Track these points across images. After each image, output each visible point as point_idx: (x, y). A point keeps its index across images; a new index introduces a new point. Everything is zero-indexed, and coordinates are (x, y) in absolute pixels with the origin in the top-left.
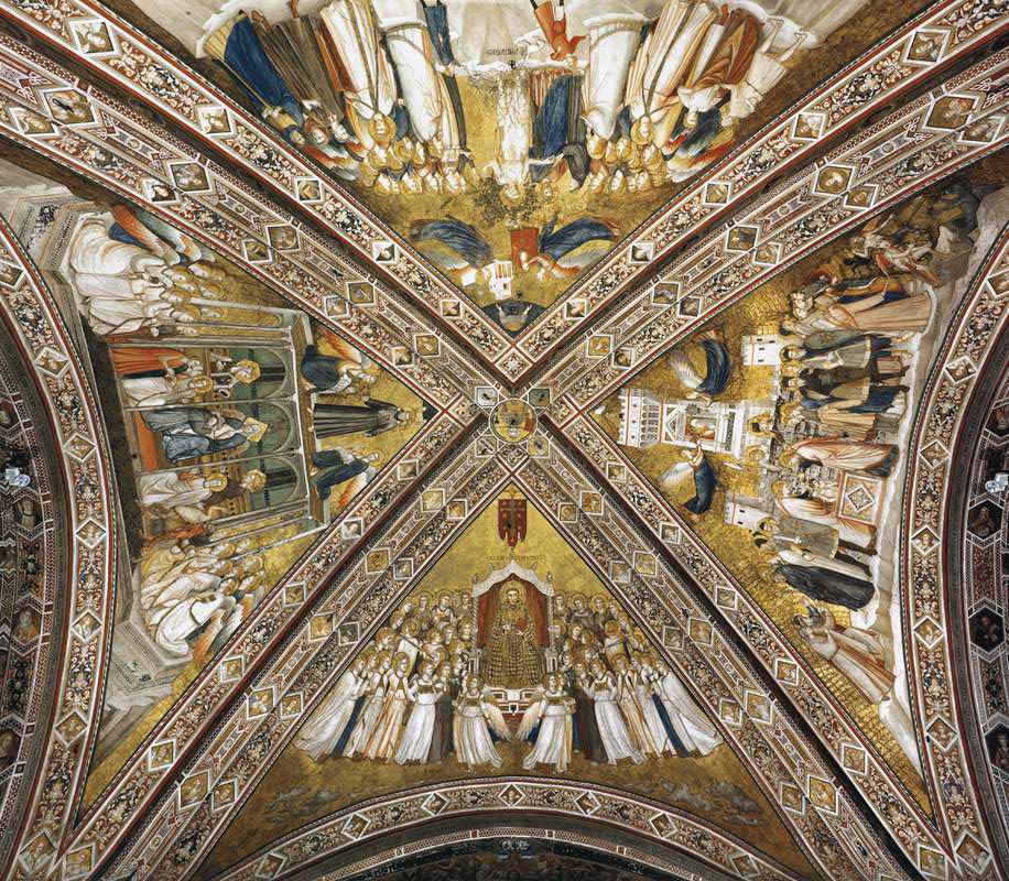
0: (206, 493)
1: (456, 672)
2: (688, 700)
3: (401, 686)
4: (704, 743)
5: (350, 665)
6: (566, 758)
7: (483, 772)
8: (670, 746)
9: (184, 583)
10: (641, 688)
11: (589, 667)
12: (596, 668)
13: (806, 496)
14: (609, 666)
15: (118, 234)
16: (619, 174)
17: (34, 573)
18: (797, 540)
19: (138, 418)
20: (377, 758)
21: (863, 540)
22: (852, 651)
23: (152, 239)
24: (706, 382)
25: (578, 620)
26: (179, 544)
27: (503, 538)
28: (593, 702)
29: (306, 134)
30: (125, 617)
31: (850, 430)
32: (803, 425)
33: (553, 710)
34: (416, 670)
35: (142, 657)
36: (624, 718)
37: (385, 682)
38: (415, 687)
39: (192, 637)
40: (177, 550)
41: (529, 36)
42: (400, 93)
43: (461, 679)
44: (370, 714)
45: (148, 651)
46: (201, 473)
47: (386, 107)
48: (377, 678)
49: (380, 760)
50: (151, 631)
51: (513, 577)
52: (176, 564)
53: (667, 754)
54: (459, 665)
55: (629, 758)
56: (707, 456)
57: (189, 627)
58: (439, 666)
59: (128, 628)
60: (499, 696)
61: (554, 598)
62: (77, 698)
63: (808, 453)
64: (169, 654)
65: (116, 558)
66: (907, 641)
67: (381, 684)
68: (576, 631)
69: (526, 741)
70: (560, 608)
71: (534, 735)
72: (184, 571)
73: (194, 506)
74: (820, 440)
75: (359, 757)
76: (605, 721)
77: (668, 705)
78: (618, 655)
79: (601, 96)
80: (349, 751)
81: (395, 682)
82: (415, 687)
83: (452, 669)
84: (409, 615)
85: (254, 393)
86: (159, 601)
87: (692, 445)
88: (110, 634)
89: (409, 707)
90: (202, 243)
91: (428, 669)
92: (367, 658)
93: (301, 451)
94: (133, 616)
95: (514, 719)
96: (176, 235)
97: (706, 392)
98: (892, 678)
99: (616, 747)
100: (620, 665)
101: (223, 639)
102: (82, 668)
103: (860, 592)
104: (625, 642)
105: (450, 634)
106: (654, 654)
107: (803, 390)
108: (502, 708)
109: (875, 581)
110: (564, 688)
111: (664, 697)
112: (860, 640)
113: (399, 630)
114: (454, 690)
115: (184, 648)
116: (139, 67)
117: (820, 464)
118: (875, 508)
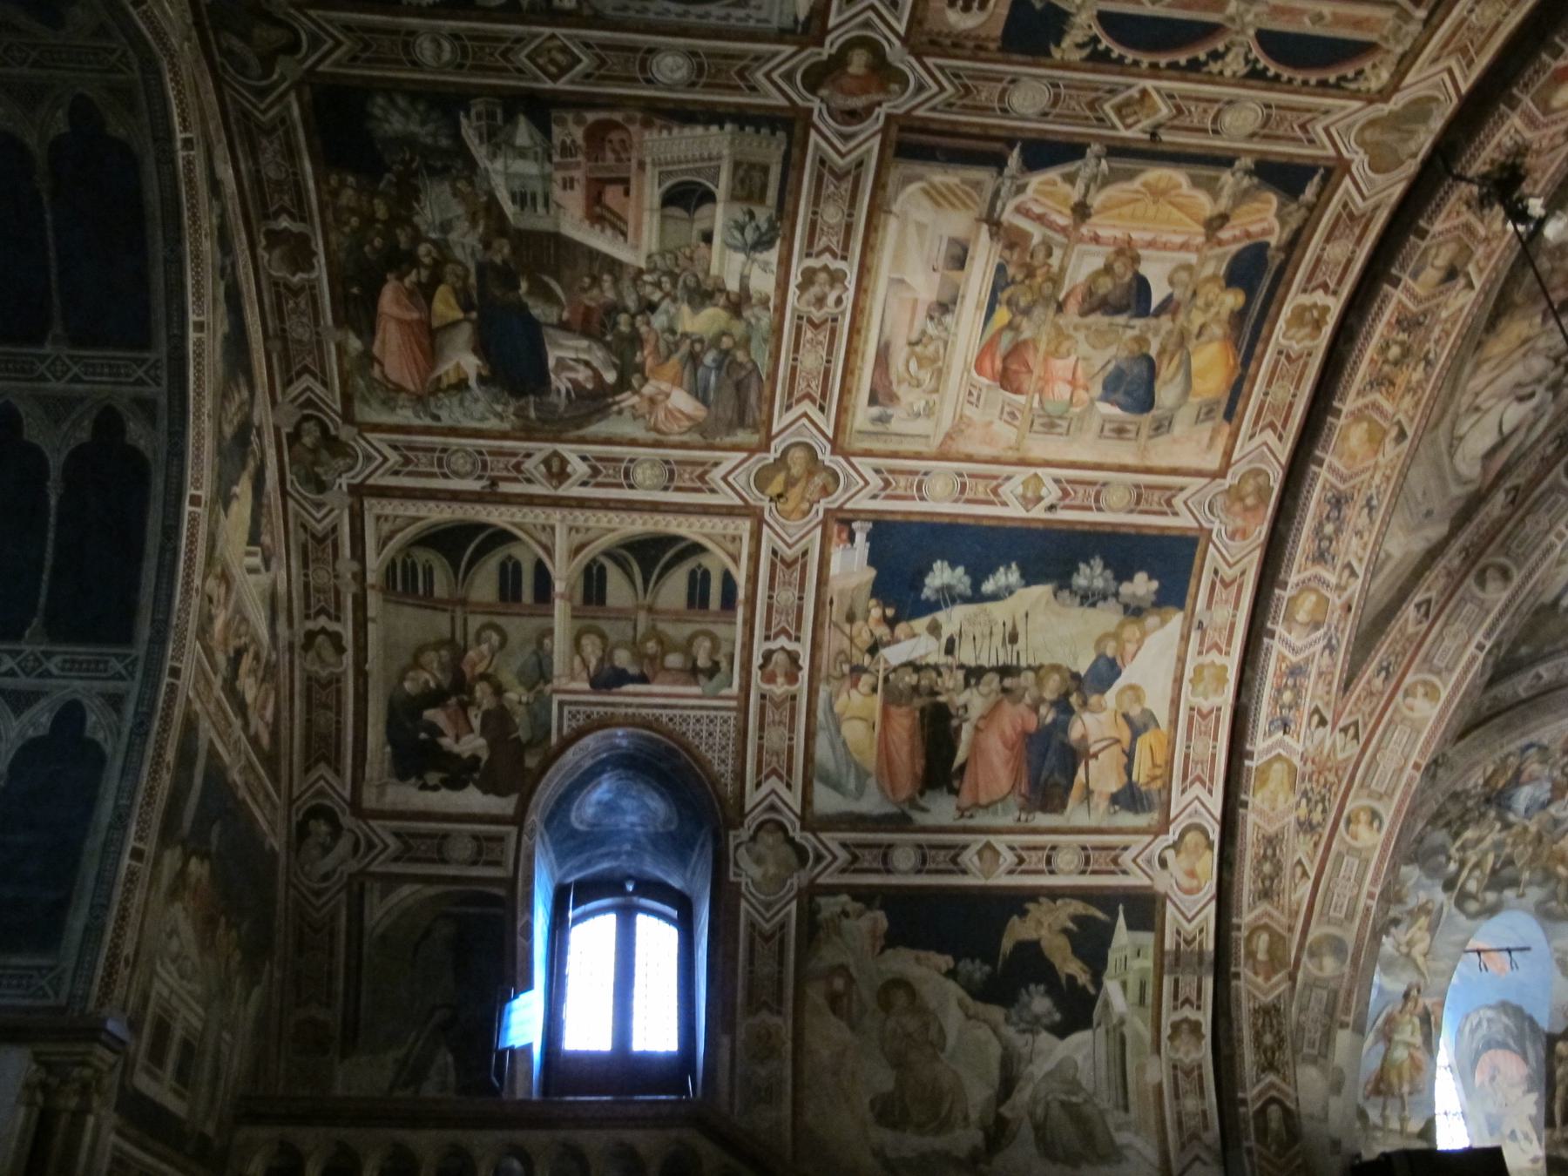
17: (1396, 363)
30: (1436, 425)
86: (1479, 400)
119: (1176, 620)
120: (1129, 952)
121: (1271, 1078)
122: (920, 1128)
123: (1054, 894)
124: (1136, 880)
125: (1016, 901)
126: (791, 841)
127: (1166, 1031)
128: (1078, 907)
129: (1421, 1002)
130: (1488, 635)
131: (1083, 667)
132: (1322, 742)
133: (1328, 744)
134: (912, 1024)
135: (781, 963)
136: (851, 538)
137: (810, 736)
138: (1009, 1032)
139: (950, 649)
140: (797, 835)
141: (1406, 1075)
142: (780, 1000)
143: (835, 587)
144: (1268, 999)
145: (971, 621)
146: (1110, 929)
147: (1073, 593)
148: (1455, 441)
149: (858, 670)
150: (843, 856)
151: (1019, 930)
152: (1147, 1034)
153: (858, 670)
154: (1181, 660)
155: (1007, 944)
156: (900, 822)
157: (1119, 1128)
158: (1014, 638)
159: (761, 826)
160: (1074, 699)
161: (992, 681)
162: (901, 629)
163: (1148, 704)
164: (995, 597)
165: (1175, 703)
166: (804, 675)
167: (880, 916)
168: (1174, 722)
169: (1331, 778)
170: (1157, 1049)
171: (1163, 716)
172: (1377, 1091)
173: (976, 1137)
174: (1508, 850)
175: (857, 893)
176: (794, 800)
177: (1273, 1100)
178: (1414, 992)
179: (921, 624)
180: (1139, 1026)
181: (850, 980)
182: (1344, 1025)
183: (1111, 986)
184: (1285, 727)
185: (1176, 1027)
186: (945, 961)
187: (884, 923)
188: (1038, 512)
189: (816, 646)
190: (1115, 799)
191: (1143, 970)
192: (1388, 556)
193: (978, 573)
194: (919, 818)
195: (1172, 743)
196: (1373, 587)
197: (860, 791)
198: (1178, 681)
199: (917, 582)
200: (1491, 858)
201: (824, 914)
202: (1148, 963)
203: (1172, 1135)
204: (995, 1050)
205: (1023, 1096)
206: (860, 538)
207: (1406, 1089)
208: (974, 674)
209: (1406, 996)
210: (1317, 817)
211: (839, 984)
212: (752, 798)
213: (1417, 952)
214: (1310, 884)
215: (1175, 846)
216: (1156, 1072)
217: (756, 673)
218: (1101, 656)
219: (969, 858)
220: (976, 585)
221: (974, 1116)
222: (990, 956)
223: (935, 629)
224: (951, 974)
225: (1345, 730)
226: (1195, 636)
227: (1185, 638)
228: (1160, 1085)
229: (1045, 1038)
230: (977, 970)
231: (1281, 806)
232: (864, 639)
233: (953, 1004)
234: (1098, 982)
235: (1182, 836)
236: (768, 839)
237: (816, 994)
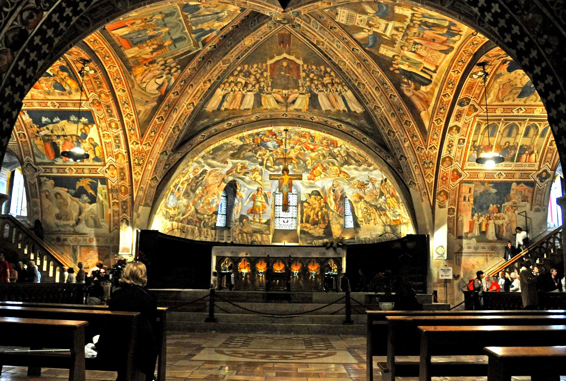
0: (151, 50)
1: (262, 86)
2: (354, 98)
3: (240, 90)
4: (358, 110)
5: (218, 86)
6: (306, 108)
8: (346, 109)
9: (150, 75)
10: (337, 93)
11: (316, 85)
12: (320, 86)
13: (414, 52)
14: (325, 86)
18: (407, 63)
19: (120, 39)
20: (233, 109)
21: (433, 69)
22: (418, 96)
24: (377, 12)
25: (313, 72)
26: (145, 65)
27: (280, 45)
28: (317, 95)
30: (133, 87)
31: (436, 39)
32: (417, 34)
33: (301, 96)
34: (246, 85)
35: (144, 97)
36: (329, 100)
37: (233, 89)
38: (246, 91)
39: (158, 89)
40: (144, 67)
43: (264, 88)
44: (229, 98)
45: (144, 95)
46: (147, 45)
48: (230, 89)
50: (144, 89)
51: (285, 59)
52: (146, 70)
53: (344, 111)
54: (262, 84)
55: (330, 110)
56: (374, 32)
57: (157, 86)
58: (255, 84)
59: (135, 90)
61: (303, 65)
62: (127, 110)
63: (417, 41)
64: (152, 94)
65: (124, 72)
66: (438, 98)
67: (232, 90)
68: (312, 75)
69: (290, 103)
70: (305, 68)
71: (294, 102)
72: (149, 72)
73: (147, 54)
74: (423, 38)
75: (226, 109)
76: (322, 99)
77: (347, 99)
78: (329, 83)
80: (223, 108)
81: (237, 89)
82: (246, 91)
83: (260, 85)
84: (240, 71)
85: (163, 21)
87: (369, 28)
88: (131, 94)
89: (243, 96)
91: (250, 86)
92: (224, 84)
93: (187, 31)
94: (136, 87)
95: (286, 98)
97: (377, 15)
98: (429, 106)
99: (325, 107)
100: (329, 86)
101: (169, 87)
102: (125, 102)
103: (427, 82)
104: (332, 80)
105: (258, 76)
106: (344, 84)
107: (419, 25)
109: (433, 80)
110: (306, 90)
111: (345, 96)
112: (422, 94)
113: (237, 75)
114: (261, 90)
115: (157, 92)
117: (422, 45)
118: (440, 61)
119: (95, 126)
120: (102, 189)
121: (125, 214)
122: (64, 220)
123: (85, 177)
124: (101, 175)
125: (78, 179)
126: (33, 167)
127: (112, 204)
128: (90, 180)
129: (263, 192)
130: (172, 125)
131: (79, 134)
132: (139, 147)
133: (141, 148)
134: (61, 201)
135: (36, 189)
136: (24, 114)
137: (32, 148)
138: (80, 203)
139: (52, 132)
140: (34, 166)
141: (261, 209)
142: (37, 196)
143: (26, 122)
144: (124, 200)
145: (54, 127)
146: (97, 184)
147: (72, 121)
149: (36, 137)
150: (43, 170)
151: (79, 184)
152: (108, 204)
153: (36, 137)
154: (99, 133)
155: (77, 187)
156: (53, 164)
157: (102, 222)
158: (63, 130)
159: (27, 164)
160: (80, 141)
161: (62, 137)
162: (41, 128)
163: (95, 141)
164: (57, 122)
165: (101, 141)
166: (27, 137)
167: (52, 181)
168: (102, 145)
169: (144, 154)
170: (110, 207)
171: (99, 143)
172: (252, 212)
173: (74, 222)
174: (275, 156)
175: (47, 177)
176: (32, 160)
177: (124, 219)
178: (260, 189)
179: (45, 128)
180: (106, 203)
181: (49, 193)
182: (141, 205)
183: (99, 195)
184: (119, 147)
185: (113, 203)
186: (66, 189)
187: (53, 183)
188: (56, 108)
189: (27, 132)
190: (93, 159)
191: (105, 192)
192: (140, 111)
193: (52, 119)
194: (56, 163)
195: (102, 149)
196: (139, 117)
197: (44, 159)
198: (100, 137)
199: (41, 121)
200: (271, 158)
201: (42, 181)
202: (106, 191)
203: (112, 224)
204: (78, 207)
205: (83, 215)
206: (26, 113)
207: (261, 212)
208: (58, 137)
209: (258, 190)
210: (141, 162)
211: (47, 193)
212: (24, 160)
213: (258, 179)
214: (141, 176)
215: (108, 168)
216: (110, 211)
217: (18, 137)
218: (82, 133)
219: (67, 170)
220: (52, 120)
221: (74, 218)
222: (74, 189)
223: (48, 129)
224: (68, 192)
225: (145, 144)
226: (100, 129)
227: (98, 129)
228: (110, 215)
229: (87, 204)
230: (73, 191)
231: (123, 162)
232: (35, 131)
233: (69, 198)
234: (96, 194)
235: (109, 166)
236: (29, 167)
237: (43, 195)
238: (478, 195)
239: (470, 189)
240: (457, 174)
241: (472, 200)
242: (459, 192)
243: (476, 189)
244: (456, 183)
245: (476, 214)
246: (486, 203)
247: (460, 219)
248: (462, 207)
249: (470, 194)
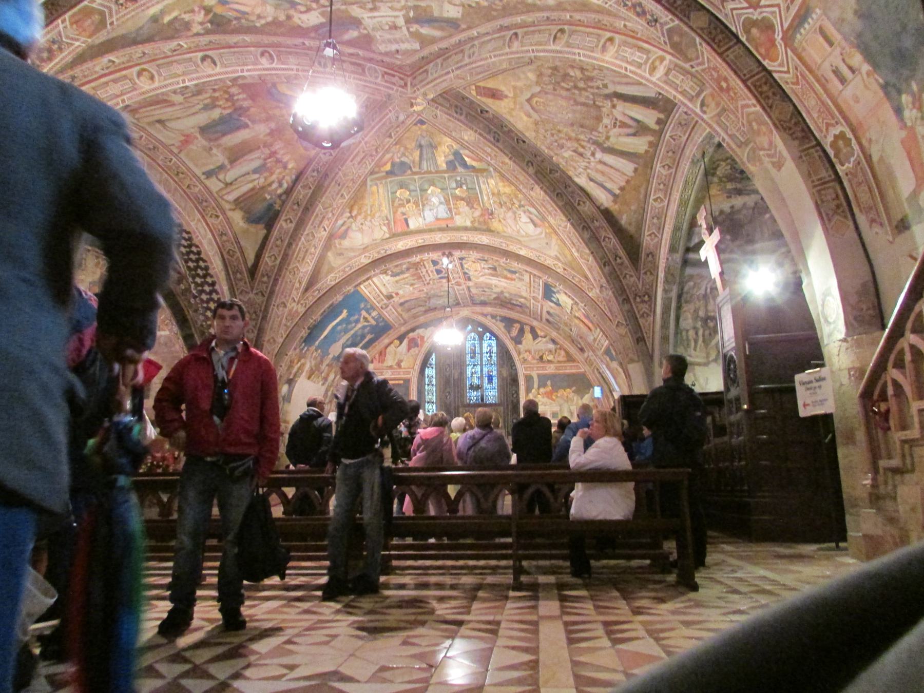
7: (654, 145)
15: (344, 236)
16: (236, 98)
23: (344, 228)
29: (280, 196)
39: (535, 225)
41: (194, 148)
42: (248, 174)
47: (257, 176)
49: (628, 182)
57: (531, 226)
60: (606, 127)
75: (622, 189)
79: (203, 118)
90: (341, 214)
96: (340, 222)
108: (615, 127)
116: (277, 246)
148: (527, 235)
238: (859, 25)
239: (822, 31)
240: (762, 31)
241: (857, 59)
242: (811, 71)
243: (835, 14)
244: (782, 56)
245: (905, 99)
246: (904, 28)
247: (875, 158)
248: (858, 112)
249: (838, 50)
